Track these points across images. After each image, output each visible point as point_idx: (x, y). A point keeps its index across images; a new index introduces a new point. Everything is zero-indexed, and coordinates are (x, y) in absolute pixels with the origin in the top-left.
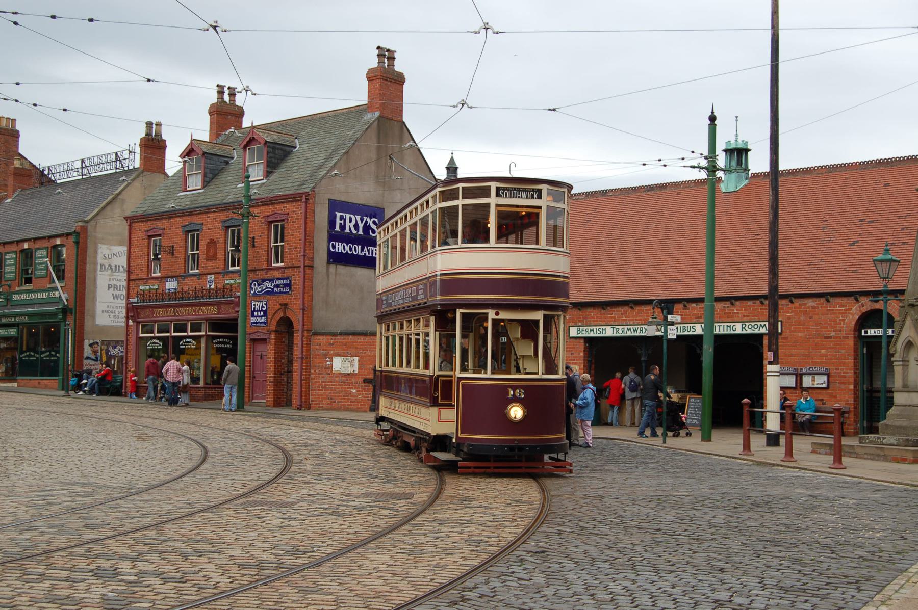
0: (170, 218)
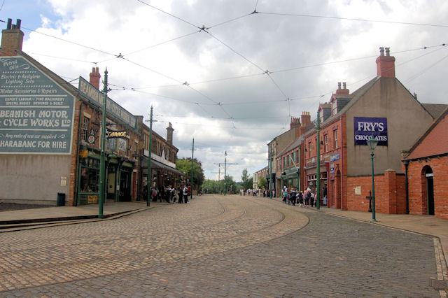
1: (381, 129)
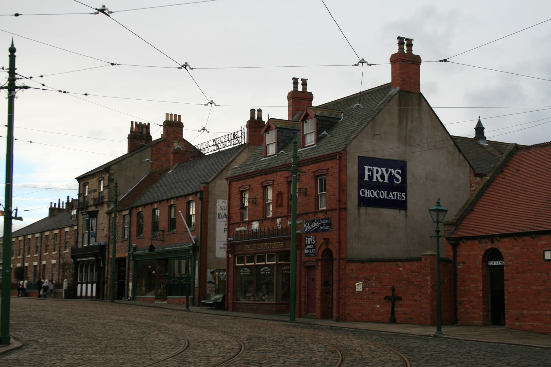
0: (253, 177)
1: (398, 180)
